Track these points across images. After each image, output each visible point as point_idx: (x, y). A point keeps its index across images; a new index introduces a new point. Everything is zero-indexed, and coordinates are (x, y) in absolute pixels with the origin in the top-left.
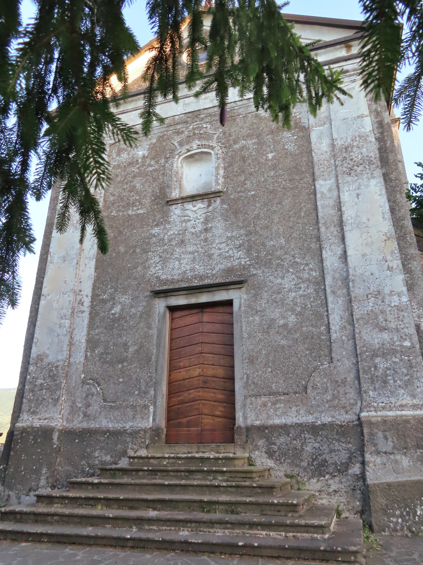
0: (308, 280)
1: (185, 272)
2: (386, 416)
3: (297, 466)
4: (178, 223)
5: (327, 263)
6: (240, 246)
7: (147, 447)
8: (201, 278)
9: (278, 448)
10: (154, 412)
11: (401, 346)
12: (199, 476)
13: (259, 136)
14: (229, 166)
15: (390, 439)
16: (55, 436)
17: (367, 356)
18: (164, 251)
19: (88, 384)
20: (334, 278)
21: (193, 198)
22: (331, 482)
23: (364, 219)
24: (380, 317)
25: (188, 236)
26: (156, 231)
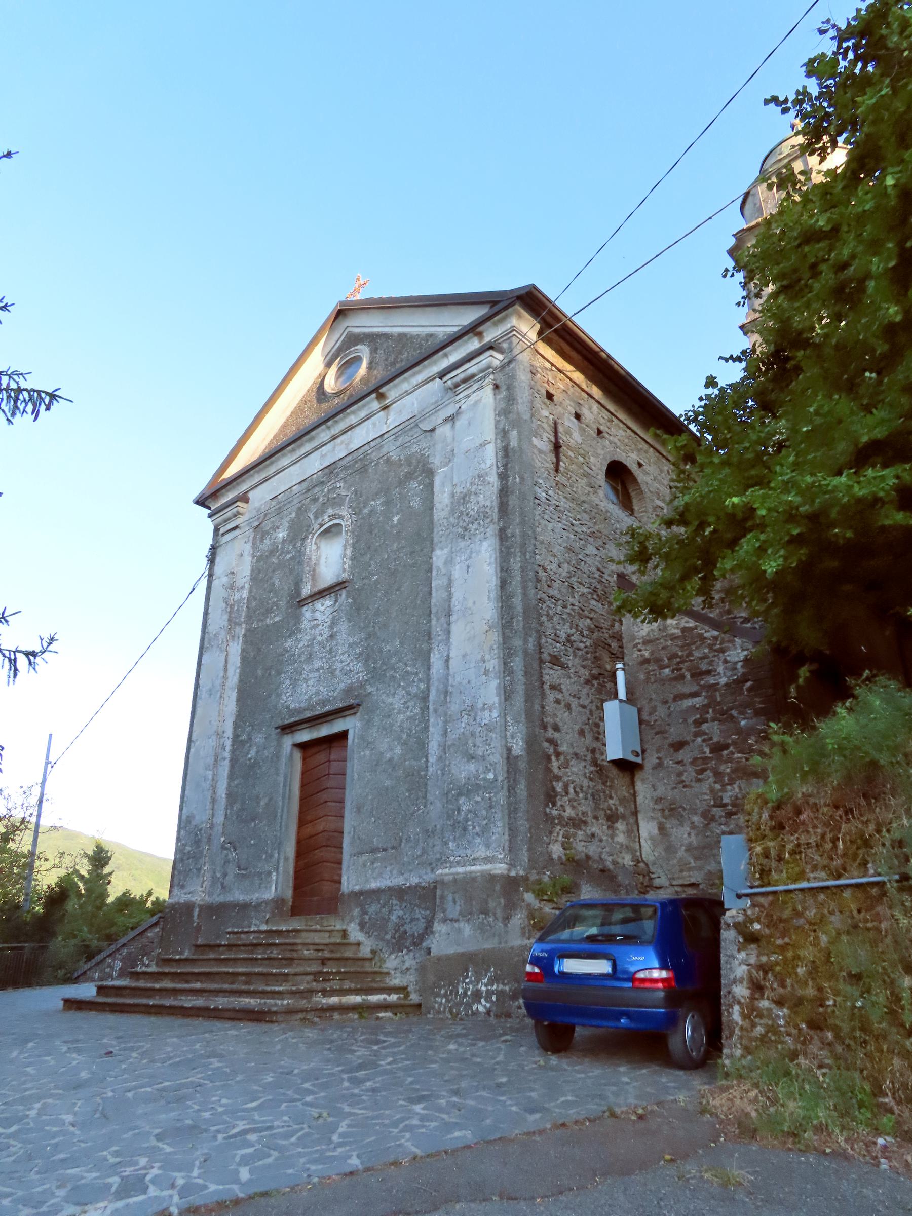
0: (416, 696)
1: (310, 698)
2: (458, 874)
3: (382, 939)
4: (308, 630)
5: (433, 671)
6: (360, 654)
7: (267, 922)
8: (324, 703)
9: (370, 919)
10: (277, 878)
11: (485, 779)
12: (260, 950)
13: (388, 491)
14: (357, 542)
15: (458, 904)
16: (196, 912)
17: (453, 796)
18: (295, 670)
19: (226, 849)
20: (438, 690)
21: (321, 594)
22: (406, 957)
23: (470, 604)
24: (470, 742)
25: (316, 647)
26: (289, 644)
